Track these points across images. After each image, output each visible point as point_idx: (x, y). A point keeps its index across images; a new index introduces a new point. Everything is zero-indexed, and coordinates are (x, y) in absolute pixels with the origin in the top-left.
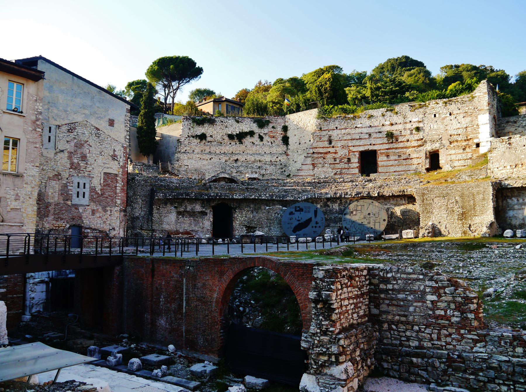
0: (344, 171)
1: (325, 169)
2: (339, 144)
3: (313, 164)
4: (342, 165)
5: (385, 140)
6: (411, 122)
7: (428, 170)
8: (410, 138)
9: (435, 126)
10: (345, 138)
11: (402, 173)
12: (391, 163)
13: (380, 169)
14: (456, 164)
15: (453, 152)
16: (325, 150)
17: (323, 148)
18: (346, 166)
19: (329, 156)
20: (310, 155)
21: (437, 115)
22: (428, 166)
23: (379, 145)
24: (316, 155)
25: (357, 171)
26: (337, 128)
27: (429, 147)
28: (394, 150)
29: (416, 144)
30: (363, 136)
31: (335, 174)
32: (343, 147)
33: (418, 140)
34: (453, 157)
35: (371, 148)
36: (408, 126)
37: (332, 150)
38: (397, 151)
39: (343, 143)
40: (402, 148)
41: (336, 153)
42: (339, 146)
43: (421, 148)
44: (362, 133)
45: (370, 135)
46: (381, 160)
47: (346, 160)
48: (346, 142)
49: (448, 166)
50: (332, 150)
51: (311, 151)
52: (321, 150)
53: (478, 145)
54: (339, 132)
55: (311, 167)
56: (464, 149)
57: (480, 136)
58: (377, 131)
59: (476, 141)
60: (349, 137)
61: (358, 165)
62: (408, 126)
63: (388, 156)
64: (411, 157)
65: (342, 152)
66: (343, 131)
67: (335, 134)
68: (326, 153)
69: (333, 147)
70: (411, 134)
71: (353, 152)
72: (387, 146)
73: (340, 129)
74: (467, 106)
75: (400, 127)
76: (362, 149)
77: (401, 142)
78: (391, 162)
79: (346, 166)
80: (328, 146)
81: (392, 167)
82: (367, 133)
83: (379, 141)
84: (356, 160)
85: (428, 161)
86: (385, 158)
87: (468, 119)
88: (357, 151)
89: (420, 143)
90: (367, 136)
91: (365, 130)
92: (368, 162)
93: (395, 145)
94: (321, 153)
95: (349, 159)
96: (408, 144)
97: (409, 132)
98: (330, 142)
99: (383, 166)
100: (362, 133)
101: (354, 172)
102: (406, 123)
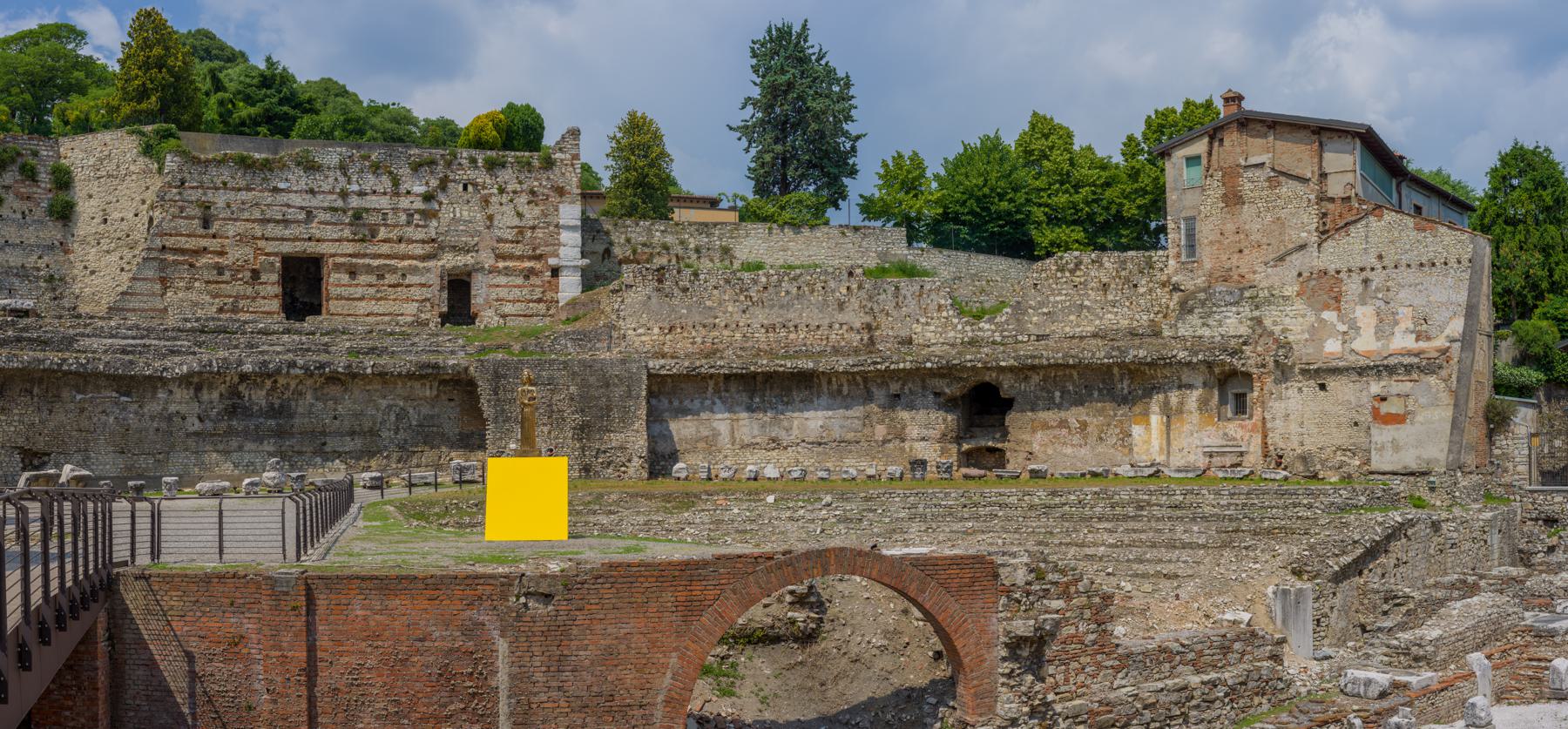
0: (241, 303)
1: (193, 296)
2: (231, 229)
3: (163, 280)
4: (238, 288)
5: (347, 233)
6: (409, 192)
7: (445, 319)
8: (410, 232)
9: (465, 213)
10: (246, 215)
11: (387, 318)
12: (359, 292)
13: (334, 306)
14: (508, 308)
15: (502, 280)
16: (191, 244)
17: (189, 236)
18: (249, 291)
19: (204, 260)
20: (154, 254)
21: (470, 188)
22: (445, 309)
23: (332, 242)
24: (171, 257)
25: (275, 305)
26: (225, 184)
27: (449, 260)
28: (367, 261)
29: (418, 250)
30: (292, 214)
31: (221, 310)
32: (242, 239)
33: (423, 242)
34: (503, 293)
35: (312, 248)
36: (404, 203)
37: (212, 244)
38: (376, 263)
39: (240, 227)
40: (388, 257)
41: (222, 254)
42: (231, 233)
43: (431, 264)
44: (289, 206)
45: (309, 213)
46: (335, 282)
47: (248, 274)
48: (249, 225)
49: (490, 313)
50: (212, 244)
51: (158, 242)
52: (185, 243)
53: (555, 272)
54: (231, 196)
55: (158, 287)
56: (527, 277)
57: (562, 251)
58: (326, 204)
59: (552, 261)
60: (257, 215)
61: (277, 290)
62: (404, 203)
63: (353, 274)
64: (407, 282)
65: (236, 254)
66: (243, 195)
67: (220, 199)
68: (198, 252)
69: (214, 236)
70: (409, 223)
71: (267, 254)
72: (349, 248)
73: (233, 189)
74: (536, 179)
75: (384, 202)
76: (287, 248)
77: (384, 241)
78: (360, 290)
79: (249, 291)
80: (201, 231)
81: (363, 303)
82: (302, 208)
83: (330, 232)
84: (274, 277)
85: (445, 295)
86: (345, 278)
87: (537, 211)
88: (276, 254)
89: (428, 248)
90: (302, 216)
91: (297, 200)
92: (302, 285)
93: (372, 249)
94: (182, 251)
95: (256, 274)
96: (402, 248)
97: (404, 218)
98: (206, 223)
99: (340, 298)
100: (289, 206)
101: (266, 309)
102: (397, 194)
